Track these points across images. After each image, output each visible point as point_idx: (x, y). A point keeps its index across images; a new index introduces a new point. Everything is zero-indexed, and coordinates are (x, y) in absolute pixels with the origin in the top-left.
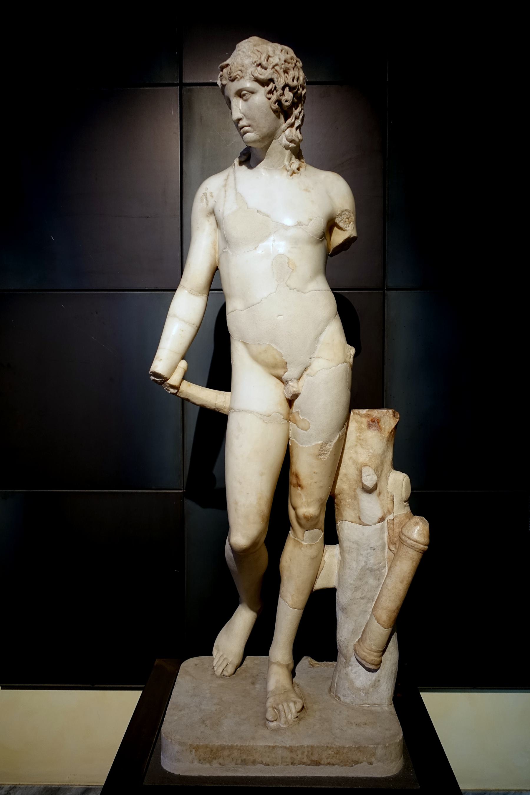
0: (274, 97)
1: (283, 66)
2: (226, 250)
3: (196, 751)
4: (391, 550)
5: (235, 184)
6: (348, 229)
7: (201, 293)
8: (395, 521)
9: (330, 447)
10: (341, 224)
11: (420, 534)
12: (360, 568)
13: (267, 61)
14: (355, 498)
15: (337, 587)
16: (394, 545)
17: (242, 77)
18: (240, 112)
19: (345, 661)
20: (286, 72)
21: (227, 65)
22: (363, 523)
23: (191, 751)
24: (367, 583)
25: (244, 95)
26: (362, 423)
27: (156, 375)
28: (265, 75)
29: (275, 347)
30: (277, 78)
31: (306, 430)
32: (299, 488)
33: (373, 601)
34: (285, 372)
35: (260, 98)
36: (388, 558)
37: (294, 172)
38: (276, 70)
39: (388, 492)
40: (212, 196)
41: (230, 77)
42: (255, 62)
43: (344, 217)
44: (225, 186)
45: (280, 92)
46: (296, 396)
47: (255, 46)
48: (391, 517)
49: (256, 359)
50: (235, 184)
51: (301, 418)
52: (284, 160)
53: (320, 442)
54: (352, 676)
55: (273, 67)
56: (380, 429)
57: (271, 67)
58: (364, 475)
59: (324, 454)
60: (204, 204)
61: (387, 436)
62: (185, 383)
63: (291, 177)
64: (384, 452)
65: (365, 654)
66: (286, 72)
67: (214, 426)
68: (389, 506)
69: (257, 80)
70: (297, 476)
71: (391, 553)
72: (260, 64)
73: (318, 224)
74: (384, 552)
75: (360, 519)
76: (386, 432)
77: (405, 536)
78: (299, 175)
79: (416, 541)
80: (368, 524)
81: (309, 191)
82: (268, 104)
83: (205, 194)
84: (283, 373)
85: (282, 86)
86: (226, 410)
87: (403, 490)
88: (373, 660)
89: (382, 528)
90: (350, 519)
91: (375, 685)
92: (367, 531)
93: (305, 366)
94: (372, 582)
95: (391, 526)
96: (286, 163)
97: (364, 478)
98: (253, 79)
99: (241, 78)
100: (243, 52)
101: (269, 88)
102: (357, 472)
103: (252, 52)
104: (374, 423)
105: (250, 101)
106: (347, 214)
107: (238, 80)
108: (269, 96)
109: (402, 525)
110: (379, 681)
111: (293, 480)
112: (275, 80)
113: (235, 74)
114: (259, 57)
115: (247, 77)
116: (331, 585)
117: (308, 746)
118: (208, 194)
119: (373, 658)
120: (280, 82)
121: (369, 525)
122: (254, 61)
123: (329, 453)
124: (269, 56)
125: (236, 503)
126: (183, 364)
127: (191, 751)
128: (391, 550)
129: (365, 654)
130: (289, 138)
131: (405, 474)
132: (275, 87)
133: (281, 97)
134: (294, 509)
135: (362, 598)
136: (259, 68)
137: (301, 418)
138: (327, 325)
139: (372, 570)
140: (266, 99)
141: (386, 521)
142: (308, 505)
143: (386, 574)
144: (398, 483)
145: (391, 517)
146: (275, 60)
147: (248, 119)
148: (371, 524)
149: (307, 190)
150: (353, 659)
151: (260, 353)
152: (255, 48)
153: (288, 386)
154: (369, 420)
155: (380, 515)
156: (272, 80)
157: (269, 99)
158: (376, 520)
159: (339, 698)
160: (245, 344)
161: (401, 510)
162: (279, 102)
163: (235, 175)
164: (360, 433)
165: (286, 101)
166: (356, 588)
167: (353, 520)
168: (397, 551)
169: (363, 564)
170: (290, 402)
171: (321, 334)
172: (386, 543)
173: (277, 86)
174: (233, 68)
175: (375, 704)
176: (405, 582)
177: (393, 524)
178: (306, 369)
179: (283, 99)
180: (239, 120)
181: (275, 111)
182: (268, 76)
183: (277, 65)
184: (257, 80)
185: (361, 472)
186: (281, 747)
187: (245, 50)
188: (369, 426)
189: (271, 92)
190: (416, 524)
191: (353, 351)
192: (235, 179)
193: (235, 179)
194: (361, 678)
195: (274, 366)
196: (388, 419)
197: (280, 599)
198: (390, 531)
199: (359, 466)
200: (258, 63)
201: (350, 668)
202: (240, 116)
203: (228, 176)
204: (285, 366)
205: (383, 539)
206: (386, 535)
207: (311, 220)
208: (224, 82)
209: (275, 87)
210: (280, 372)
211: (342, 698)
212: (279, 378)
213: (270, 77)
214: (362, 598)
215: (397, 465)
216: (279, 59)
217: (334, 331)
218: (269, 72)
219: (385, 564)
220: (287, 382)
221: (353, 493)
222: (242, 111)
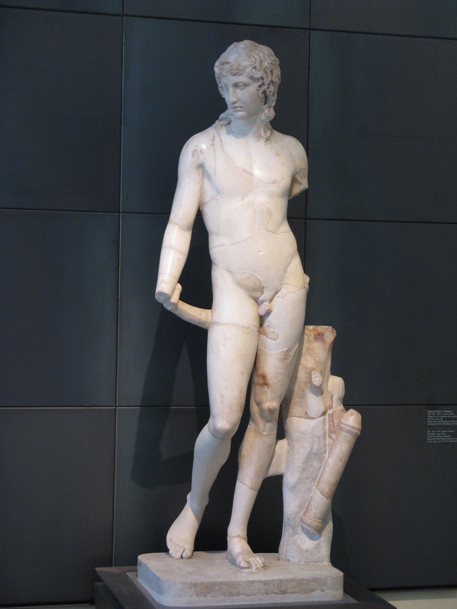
2: (217, 198)
3: (195, 587)
4: (331, 438)
5: (222, 145)
6: (303, 182)
7: (189, 230)
8: (334, 415)
9: (292, 353)
10: (299, 179)
11: (355, 422)
12: (307, 453)
14: (303, 396)
15: (285, 472)
16: (334, 434)
17: (241, 74)
18: (236, 97)
19: (292, 531)
22: (310, 417)
23: (191, 588)
24: (311, 465)
26: (310, 336)
27: (161, 293)
28: (258, 74)
29: (256, 275)
31: (275, 340)
32: (266, 387)
33: (316, 480)
34: (262, 294)
36: (328, 444)
37: (267, 139)
39: (328, 392)
42: (252, 65)
43: (301, 173)
44: (213, 145)
46: (268, 313)
47: (250, 51)
48: (330, 412)
49: (240, 284)
50: (222, 145)
51: (271, 330)
53: (286, 349)
54: (299, 542)
56: (323, 341)
57: (263, 69)
58: (313, 376)
59: (287, 358)
60: (196, 158)
61: (328, 347)
62: (181, 302)
64: (326, 359)
65: (311, 521)
67: (198, 338)
68: (329, 403)
69: (252, 78)
70: (264, 377)
71: (331, 440)
72: (255, 68)
73: (285, 182)
74: (325, 440)
75: (306, 413)
76: (328, 344)
77: (344, 424)
79: (352, 427)
80: (313, 417)
81: (279, 155)
84: (259, 296)
86: (207, 324)
87: (341, 390)
88: (316, 525)
89: (324, 420)
90: (298, 415)
91: (317, 547)
92: (312, 423)
93: (277, 290)
94: (316, 464)
95: (331, 418)
96: (263, 133)
97: (313, 379)
100: (242, 56)
101: (259, 83)
102: (306, 375)
104: (319, 337)
106: (303, 171)
107: (239, 76)
109: (340, 417)
110: (320, 544)
111: (256, 380)
113: (236, 72)
115: (245, 75)
116: (279, 472)
117: (278, 580)
118: (199, 151)
119: (316, 523)
121: (314, 419)
123: (291, 358)
124: (262, 61)
125: (222, 397)
126: (179, 287)
127: (191, 588)
128: (331, 438)
129: (311, 521)
131: (340, 378)
134: (259, 404)
135: (307, 478)
136: (254, 70)
137: (271, 330)
138: (292, 259)
139: (316, 455)
140: (256, 90)
141: (327, 414)
142: (272, 400)
143: (327, 457)
144: (336, 384)
145: (330, 412)
146: (266, 64)
148: (316, 417)
149: (278, 154)
150: (299, 529)
151: (244, 279)
153: (263, 305)
154: (316, 333)
155: (322, 409)
156: (262, 78)
158: (320, 414)
159: (289, 560)
160: (229, 271)
161: (338, 407)
163: (220, 136)
164: (309, 344)
166: (303, 469)
167: (301, 416)
168: (337, 437)
169: (309, 449)
170: (262, 319)
171: (288, 266)
172: (327, 432)
173: (265, 82)
175: (318, 562)
176: (343, 460)
177: (333, 417)
178: (277, 293)
180: (235, 103)
183: (266, 67)
184: (252, 78)
185: (310, 375)
186: (258, 581)
188: (316, 339)
190: (352, 414)
191: (308, 279)
194: (306, 543)
195: (254, 290)
196: (329, 334)
197: (238, 484)
198: (331, 423)
199: (308, 370)
200: (254, 66)
201: (297, 536)
202: (235, 100)
203: (214, 137)
204: (262, 289)
205: (324, 429)
206: (327, 425)
207: (283, 179)
209: (264, 82)
210: (257, 294)
211: (291, 560)
212: (256, 300)
214: (307, 478)
215: (334, 372)
216: (269, 64)
217: (296, 263)
219: (326, 449)
220: (262, 302)
221: (302, 393)
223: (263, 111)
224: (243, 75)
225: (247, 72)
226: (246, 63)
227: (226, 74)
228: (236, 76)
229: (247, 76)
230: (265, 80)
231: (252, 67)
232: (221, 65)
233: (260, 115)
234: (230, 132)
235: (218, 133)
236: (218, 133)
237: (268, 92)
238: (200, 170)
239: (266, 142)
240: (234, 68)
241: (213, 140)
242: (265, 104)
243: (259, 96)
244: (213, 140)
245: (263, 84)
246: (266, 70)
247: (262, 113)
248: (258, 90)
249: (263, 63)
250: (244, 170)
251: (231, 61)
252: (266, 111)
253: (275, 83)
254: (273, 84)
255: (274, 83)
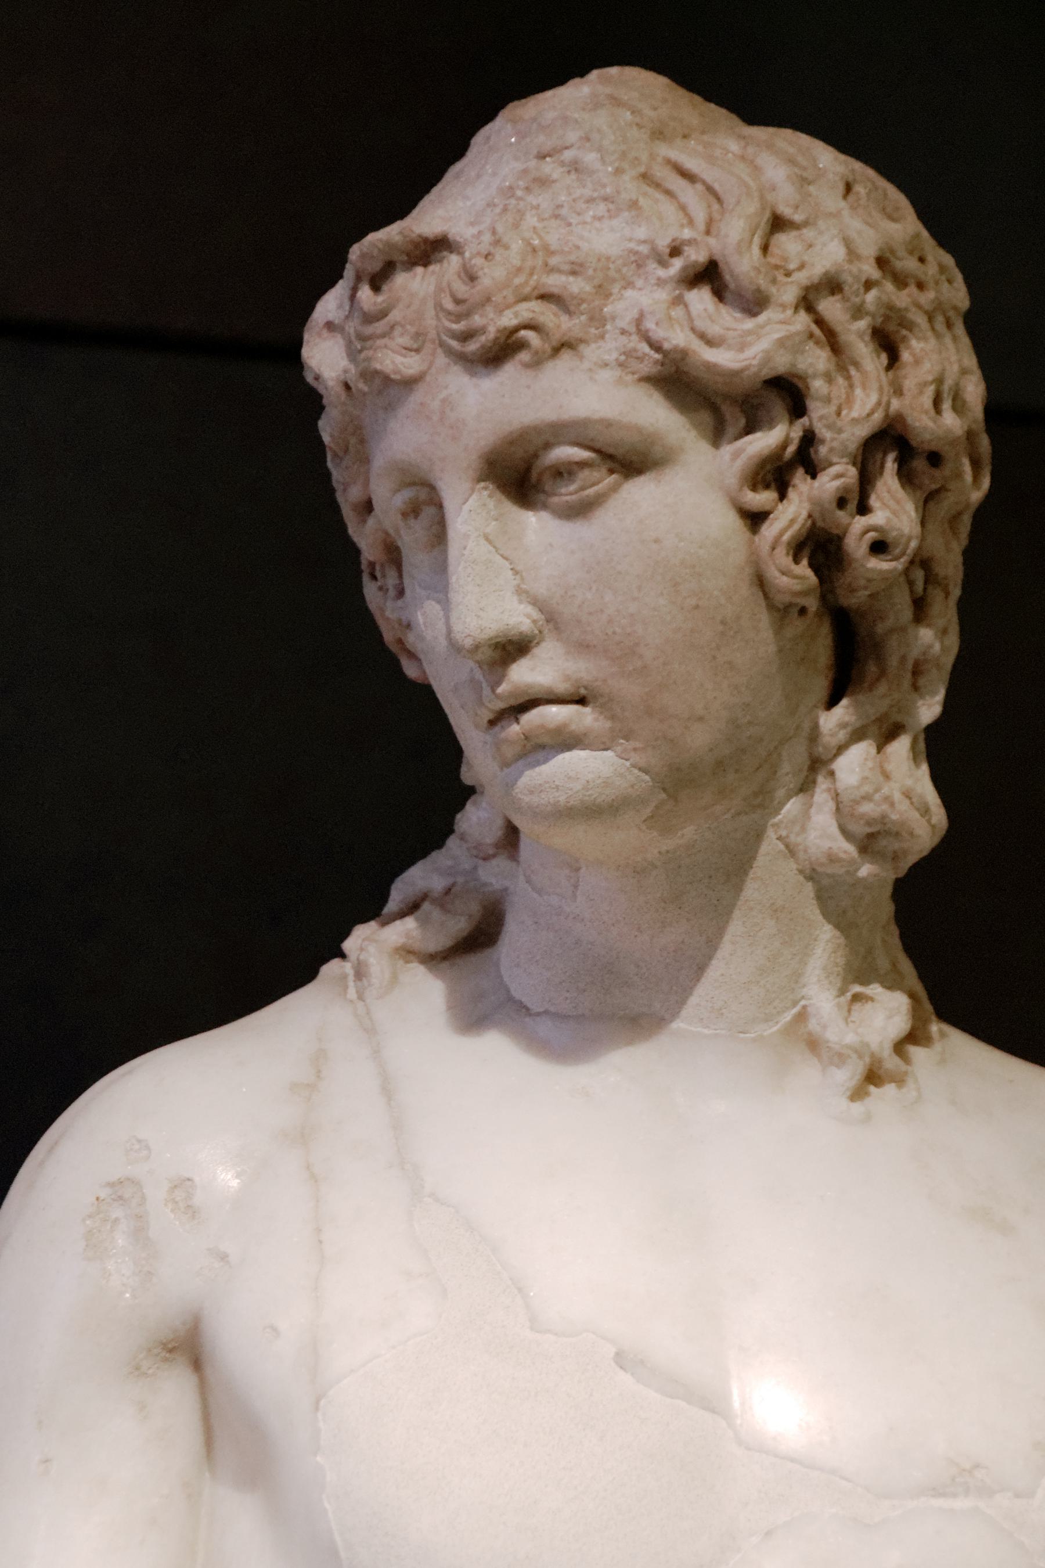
0: (791, 514)
1: (871, 296)
13: (765, 249)
17: (564, 346)
18: (520, 592)
20: (888, 343)
21: (430, 251)
25: (563, 472)
28: (743, 346)
30: (829, 379)
35: (690, 505)
37: (873, 1077)
38: (820, 322)
40: (192, 1212)
41: (466, 337)
42: (675, 251)
44: (302, 1136)
45: (836, 477)
47: (659, 134)
52: (797, 977)
55: (807, 302)
57: (790, 294)
63: (857, 1108)
66: (888, 343)
69: (678, 381)
72: (709, 275)
78: (909, 1092)
82: (739, 557)
83: (123, 1191)
85: (863, 431)
96: (823, 1000)
98: (646, 368)
99: (557, 350)
100: (575, 167)
101: (763, 442)
103: (645, 177)
105: (606, 517)
107: (537, 363)
108: (762, 499)
112: (818, 385)
113: (508, 320)
114: (700, 216)
115: (609, 348)
120: (849, 407)
122: (663, 244)
124: (778, 224)
130: (867, 808)
132: (809, 439)
133: (842, 515)
136: (701, 299)
140: (733, 521)
146: (819, 250)
147: (583, 648)
152: (665, 151)
156: (788, 393)
157: (755, 519)
162: (820, 547)
163: (376, 1053)
165: (879, 547)
173: (822, 431)
174: (491, 275)
179: (857, 532)
180: (512, 649)
181: (784, 612)
182: (767, 358)
183: (832, 285)
184: (678, 381)
187: (590, 158)
189: (776, 474)
192: (387, 1090)
193: (387, 1090)
200: (697, 256)
202: (518, 617)
203: (319, 1059)
208: (393, 359)
209: (809, 439)
213: (781, 364)
218: (777, 333)
222: (541, 588)
223: (817, 765)
224: (591, 352)
225: (626, 321)
226: (607, 237)
227: (406, 364)
228: (510, 370)
229: (626, 360)
230: (818, 413)
231: (677, 265)
232: (365, 293)
233: (792, 807)
234: (474, 1015)
235: (370, 1030)
236: (370, 1030)
237: (856, 544)
238: (175, 1389)
239: (858, 1094)
240: (486, 282)
241: (309, 1088)
242: (832, 702)
243: (761, 581)
244: (309, 1088)
245: (807, 457)
246: (830, 307)
247: (806, 787)
248: (755, 519)
249: (787, 243)
250: (621, 1359)
251: (459, 230)
252: (853, 765)
253: (935, 459)
254: (906, 476)
255: (919, 464)
